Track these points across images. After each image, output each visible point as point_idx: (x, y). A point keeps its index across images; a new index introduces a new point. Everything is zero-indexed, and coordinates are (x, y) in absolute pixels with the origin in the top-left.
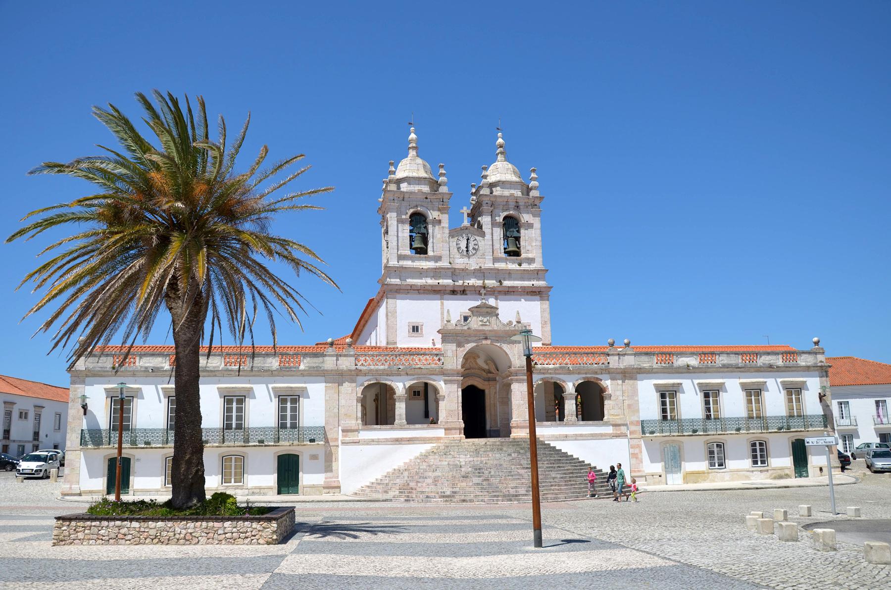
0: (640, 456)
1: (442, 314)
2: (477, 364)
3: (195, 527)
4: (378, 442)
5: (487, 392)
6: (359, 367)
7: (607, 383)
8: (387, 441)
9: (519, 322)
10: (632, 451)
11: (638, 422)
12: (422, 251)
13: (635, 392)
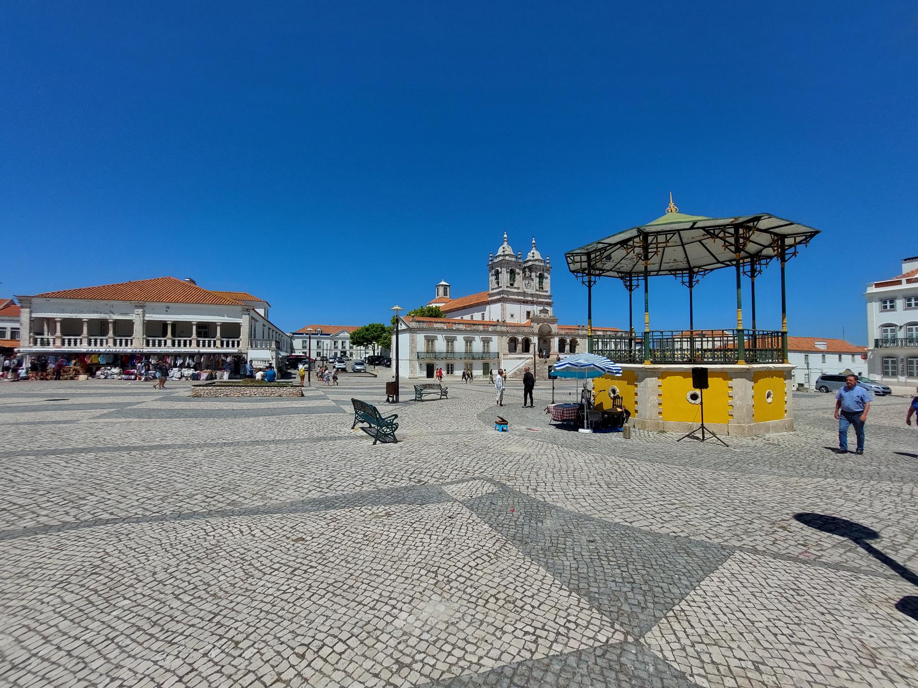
4: (514, 359)
7: (578, 340)
12: (512, 285)
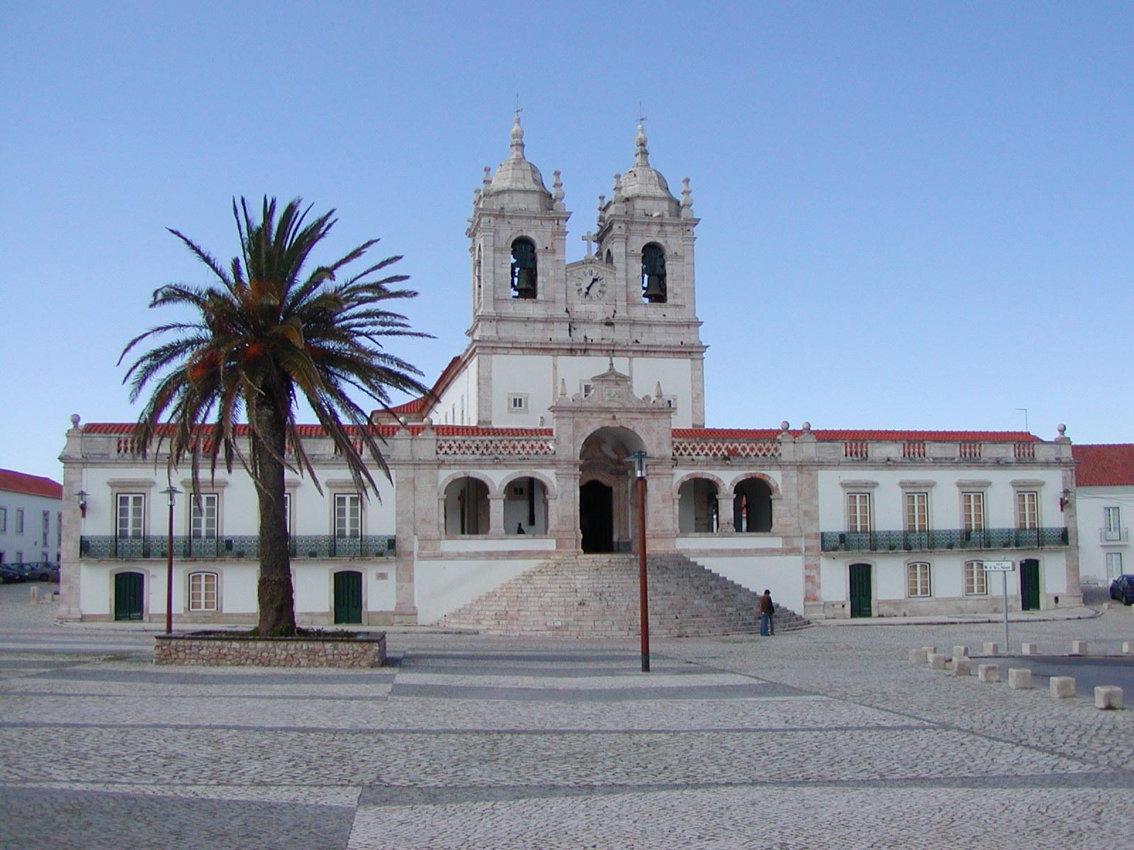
0: (816, 579)
1: (555, 383)
2: (601, 451)
3: (296, 649)
5: (615, 490)
6: (441, 456)
8: (476, 555)
9: (659, 396)
11: (817, 534)
13: (814, 494)
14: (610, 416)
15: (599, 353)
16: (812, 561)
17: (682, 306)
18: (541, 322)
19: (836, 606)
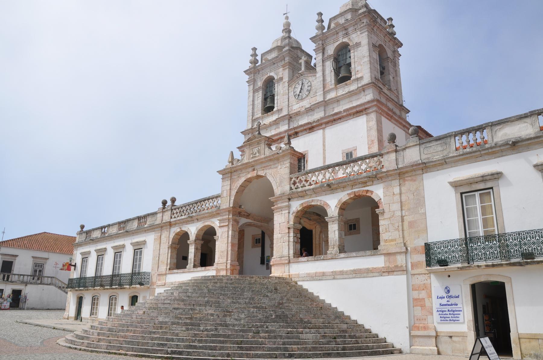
0: (427, 304)
10: (415, 294)
13: (420, 202)
14: (251, 169)
15: (305, 132)
16: (419, 280)
17: (361, 78)
18: (274, 124)
19: (454, 338)
